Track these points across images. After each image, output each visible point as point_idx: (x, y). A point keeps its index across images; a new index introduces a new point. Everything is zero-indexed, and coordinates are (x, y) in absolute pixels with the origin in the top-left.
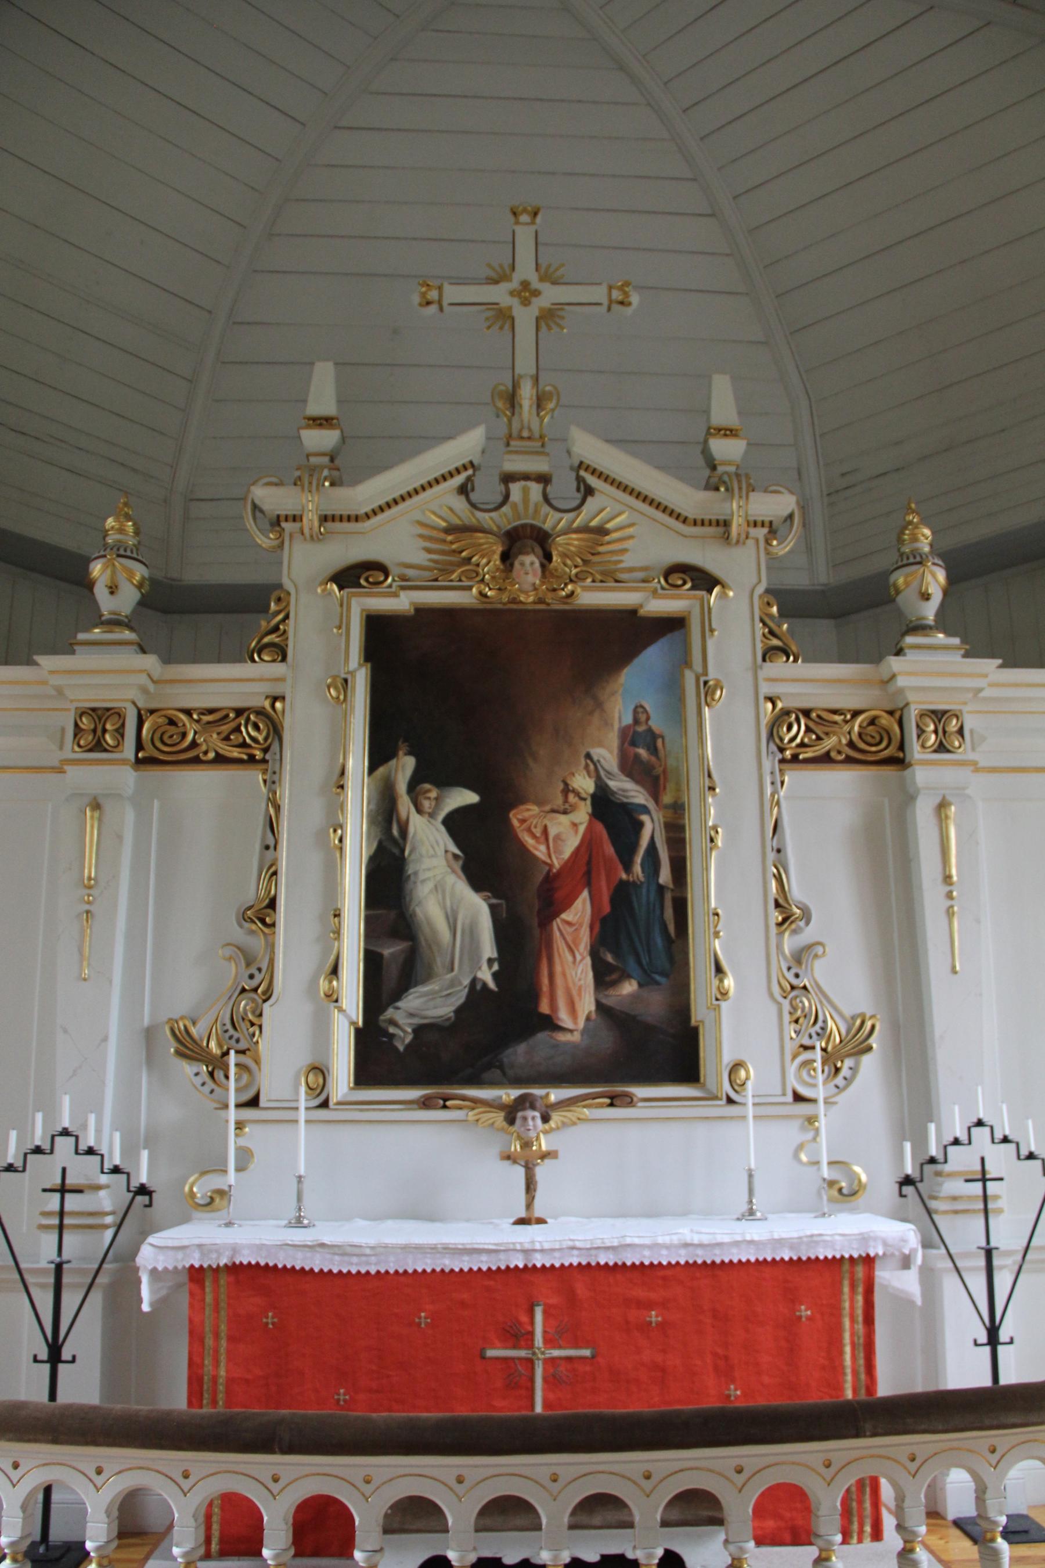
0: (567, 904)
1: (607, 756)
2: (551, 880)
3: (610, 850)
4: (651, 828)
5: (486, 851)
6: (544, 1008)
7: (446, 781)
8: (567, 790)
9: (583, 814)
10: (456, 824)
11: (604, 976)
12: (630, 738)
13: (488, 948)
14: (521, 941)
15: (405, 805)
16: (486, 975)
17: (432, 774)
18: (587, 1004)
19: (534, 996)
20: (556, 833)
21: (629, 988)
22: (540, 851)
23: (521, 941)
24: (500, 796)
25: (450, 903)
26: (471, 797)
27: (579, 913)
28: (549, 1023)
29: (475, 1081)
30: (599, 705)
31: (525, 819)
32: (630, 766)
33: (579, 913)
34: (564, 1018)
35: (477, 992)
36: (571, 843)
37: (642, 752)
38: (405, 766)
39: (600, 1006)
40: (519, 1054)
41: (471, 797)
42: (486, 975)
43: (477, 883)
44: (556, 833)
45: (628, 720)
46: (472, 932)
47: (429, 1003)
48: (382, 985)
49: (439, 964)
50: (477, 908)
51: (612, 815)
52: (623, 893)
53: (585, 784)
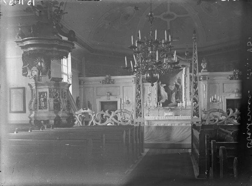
0: (173, 93)
1: (176, 81)
2: (172, 91)
3: (177, 89)
4: (180, 87)
5: (167, 89)
6: (171, 101)
7: (164, 84)
8: (173, 84)
9: (174, 86)
10: (164, 87)
11: (176, 99)
12: (178, 80)
13: (167, 97)
14: (169, 96)
15: (160, 86)
16: (167, 99)
17: (162, 83)
18: (175, 101)
19: (171, 100)
20: (172, 88)
21: (178, 99)
22: (171, 89)
23: (169, 96)
24: (168, 85)
25: (163, 93)
26: (165, 85)
27: (174, 93)
28: (172, 102)
29: (166, 107)
30: (176, 77)
31: (170, 86)
32: (178, 82)
33: (174, 93)
34: (173, 102)
35: (166, 100)
36: (174, 88)
37: (179, 81)
38: (160, 82)
39: (176, 101)
40: (170, 105)
41: (165, 85)
42: (167, 99)
43: (166, 92)
44: (172, 88)
45: (178, 78)
46: (166, 95)
47: (163, 101)
48: (159, 100)
49: (163, 98)
50: (166, 94)
51: (176, 85)
52: (178, 92)
53: (175, 84)
